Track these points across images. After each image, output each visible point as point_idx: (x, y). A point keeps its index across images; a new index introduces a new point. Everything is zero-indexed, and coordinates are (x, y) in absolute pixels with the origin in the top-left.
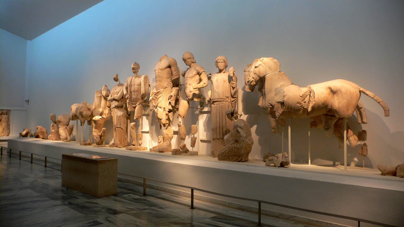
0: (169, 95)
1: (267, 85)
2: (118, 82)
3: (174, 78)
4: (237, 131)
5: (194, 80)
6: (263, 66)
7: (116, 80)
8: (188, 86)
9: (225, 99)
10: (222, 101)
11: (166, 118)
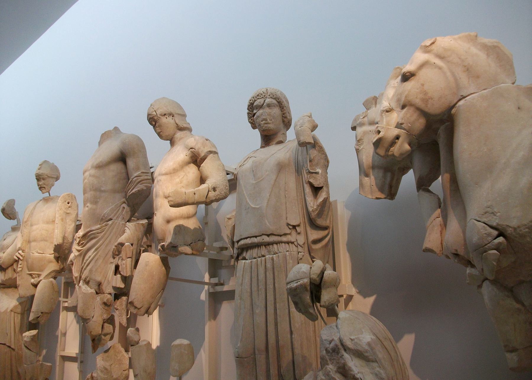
0: (116, 244)
1: (467, 146)
2: (14, 223)
3: (134, 191)
4: (344, 371)
5: (178, 180)
6: (440, 68)
9: (285, 234)
10: (272, 243)
11: (105, 316)
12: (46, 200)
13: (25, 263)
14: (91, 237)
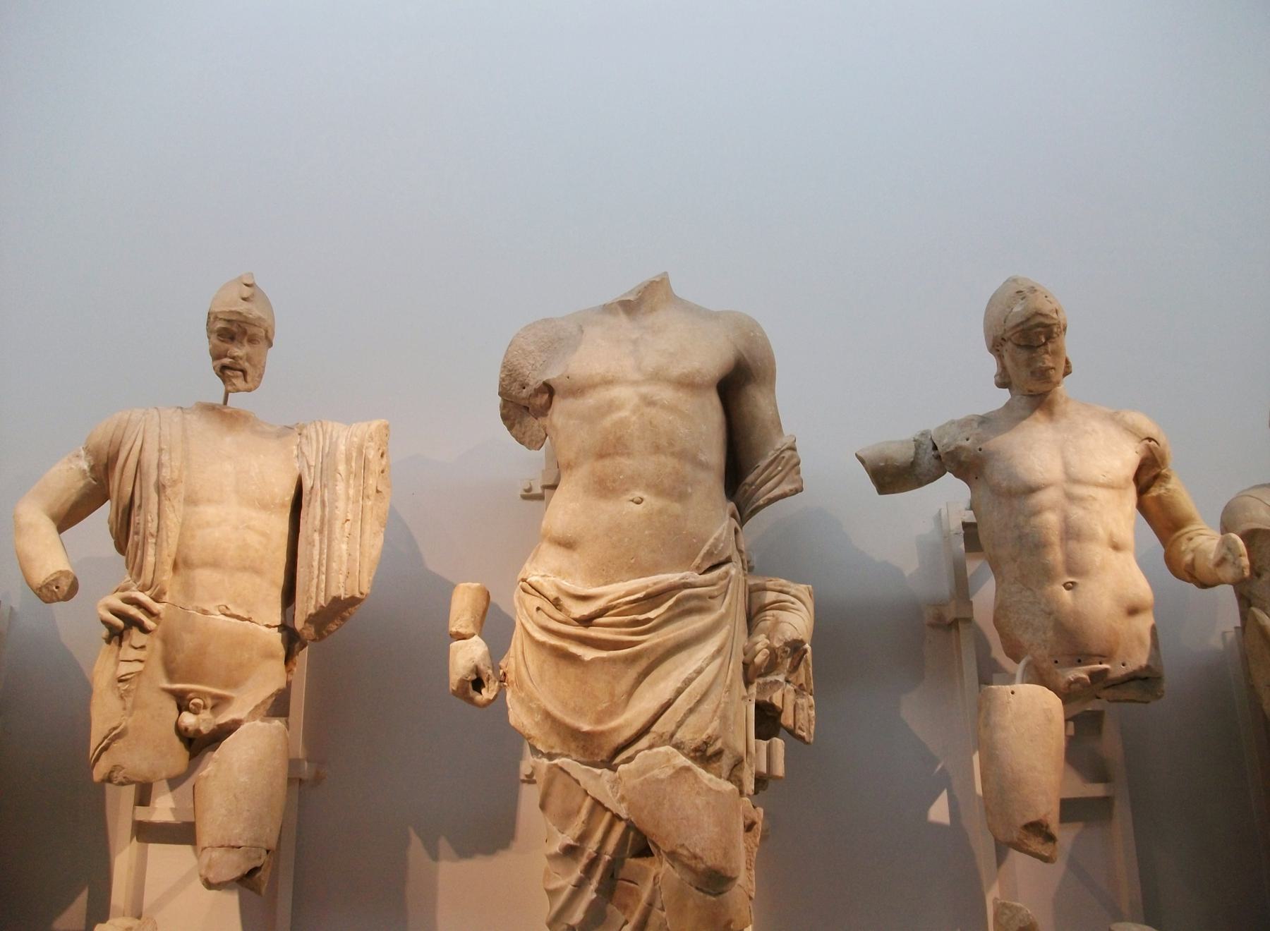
8: (1097, 553)
12: (221, 413)
13: (158, 645)
14: (693, 604)
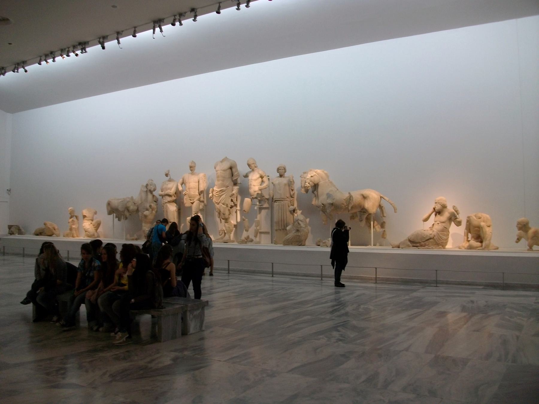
1: (320, 189)
4: (298, 223)
7: (167, 175)
8: (252, 186)
